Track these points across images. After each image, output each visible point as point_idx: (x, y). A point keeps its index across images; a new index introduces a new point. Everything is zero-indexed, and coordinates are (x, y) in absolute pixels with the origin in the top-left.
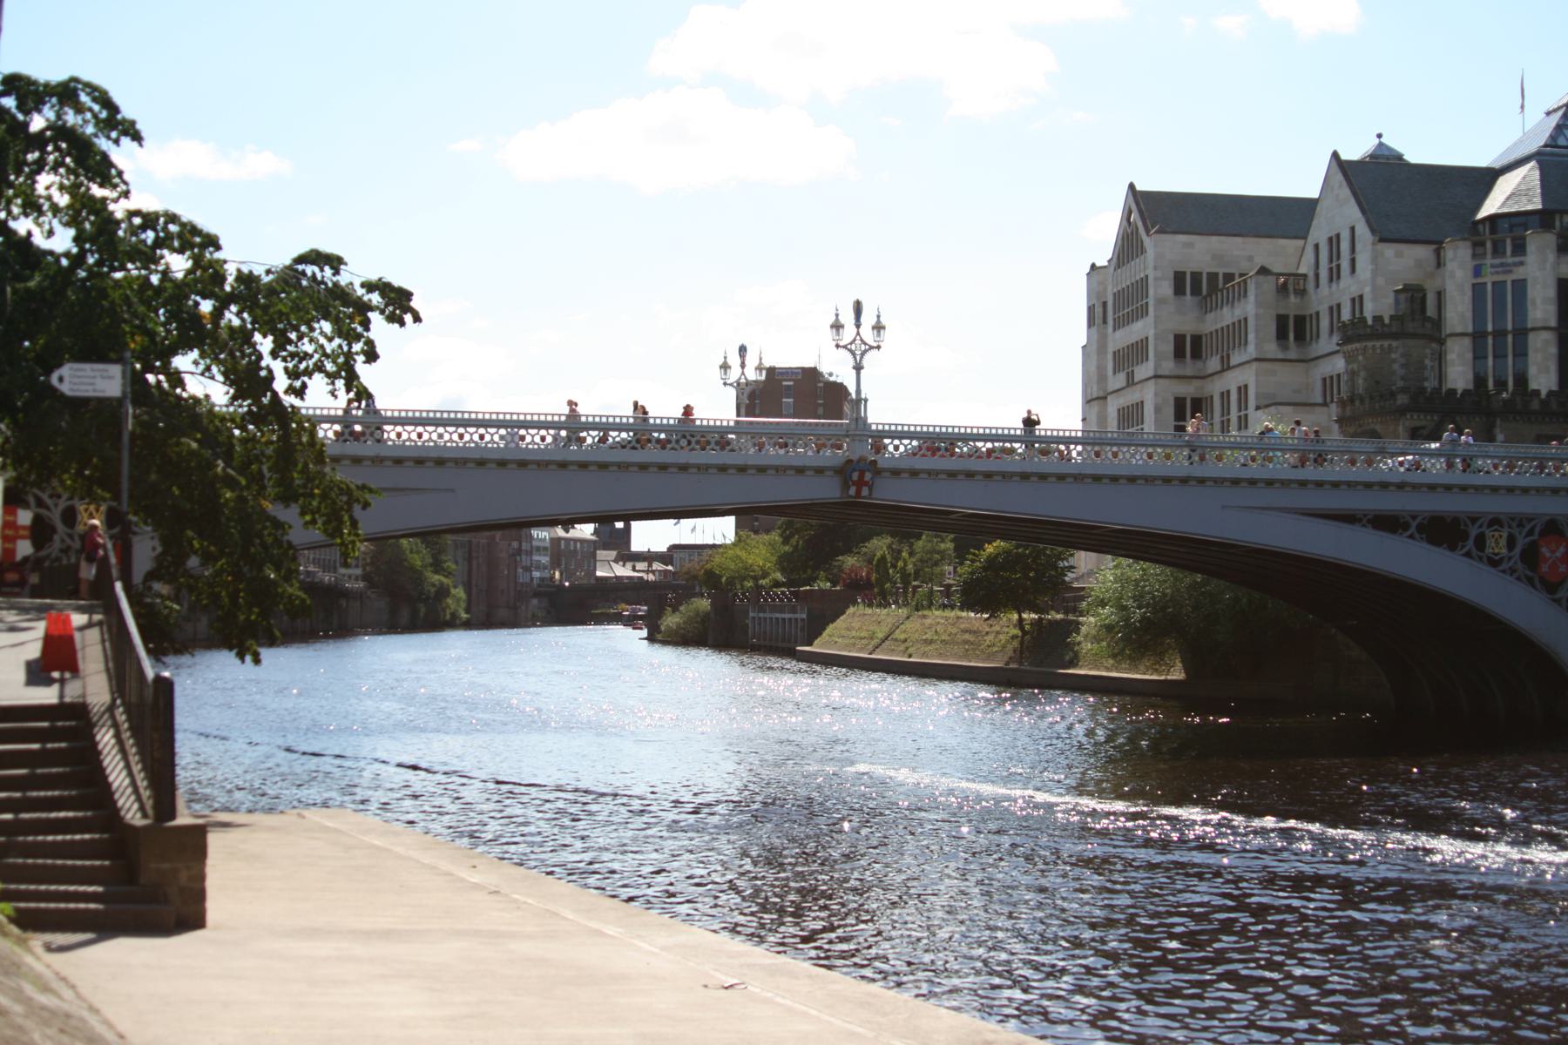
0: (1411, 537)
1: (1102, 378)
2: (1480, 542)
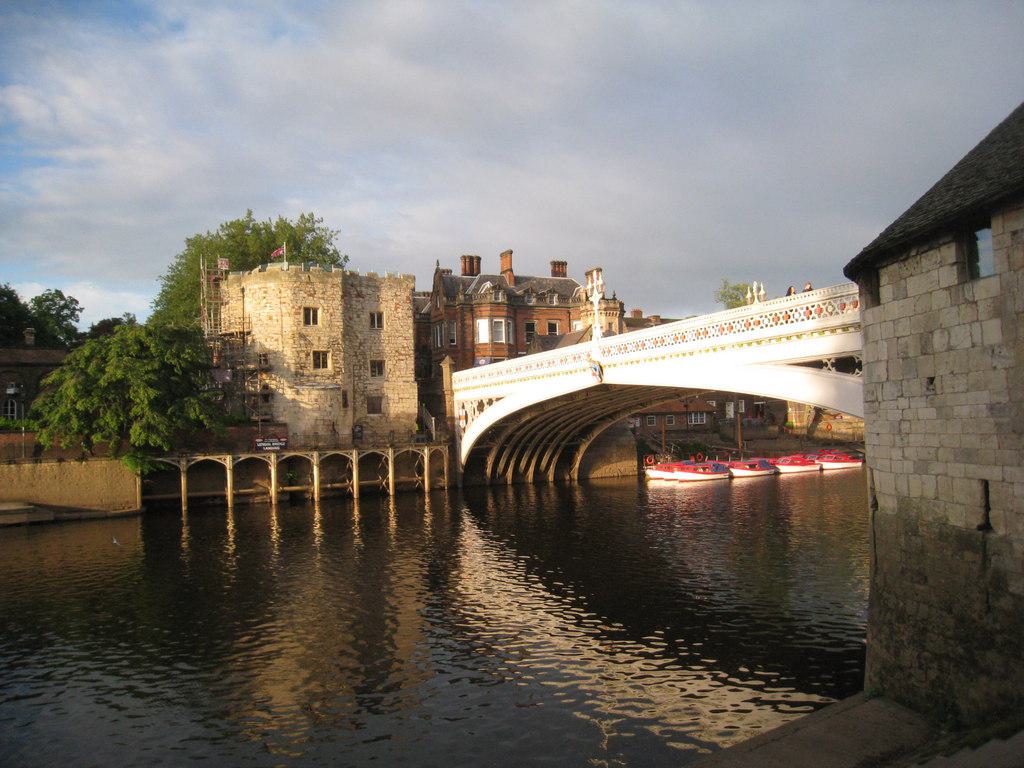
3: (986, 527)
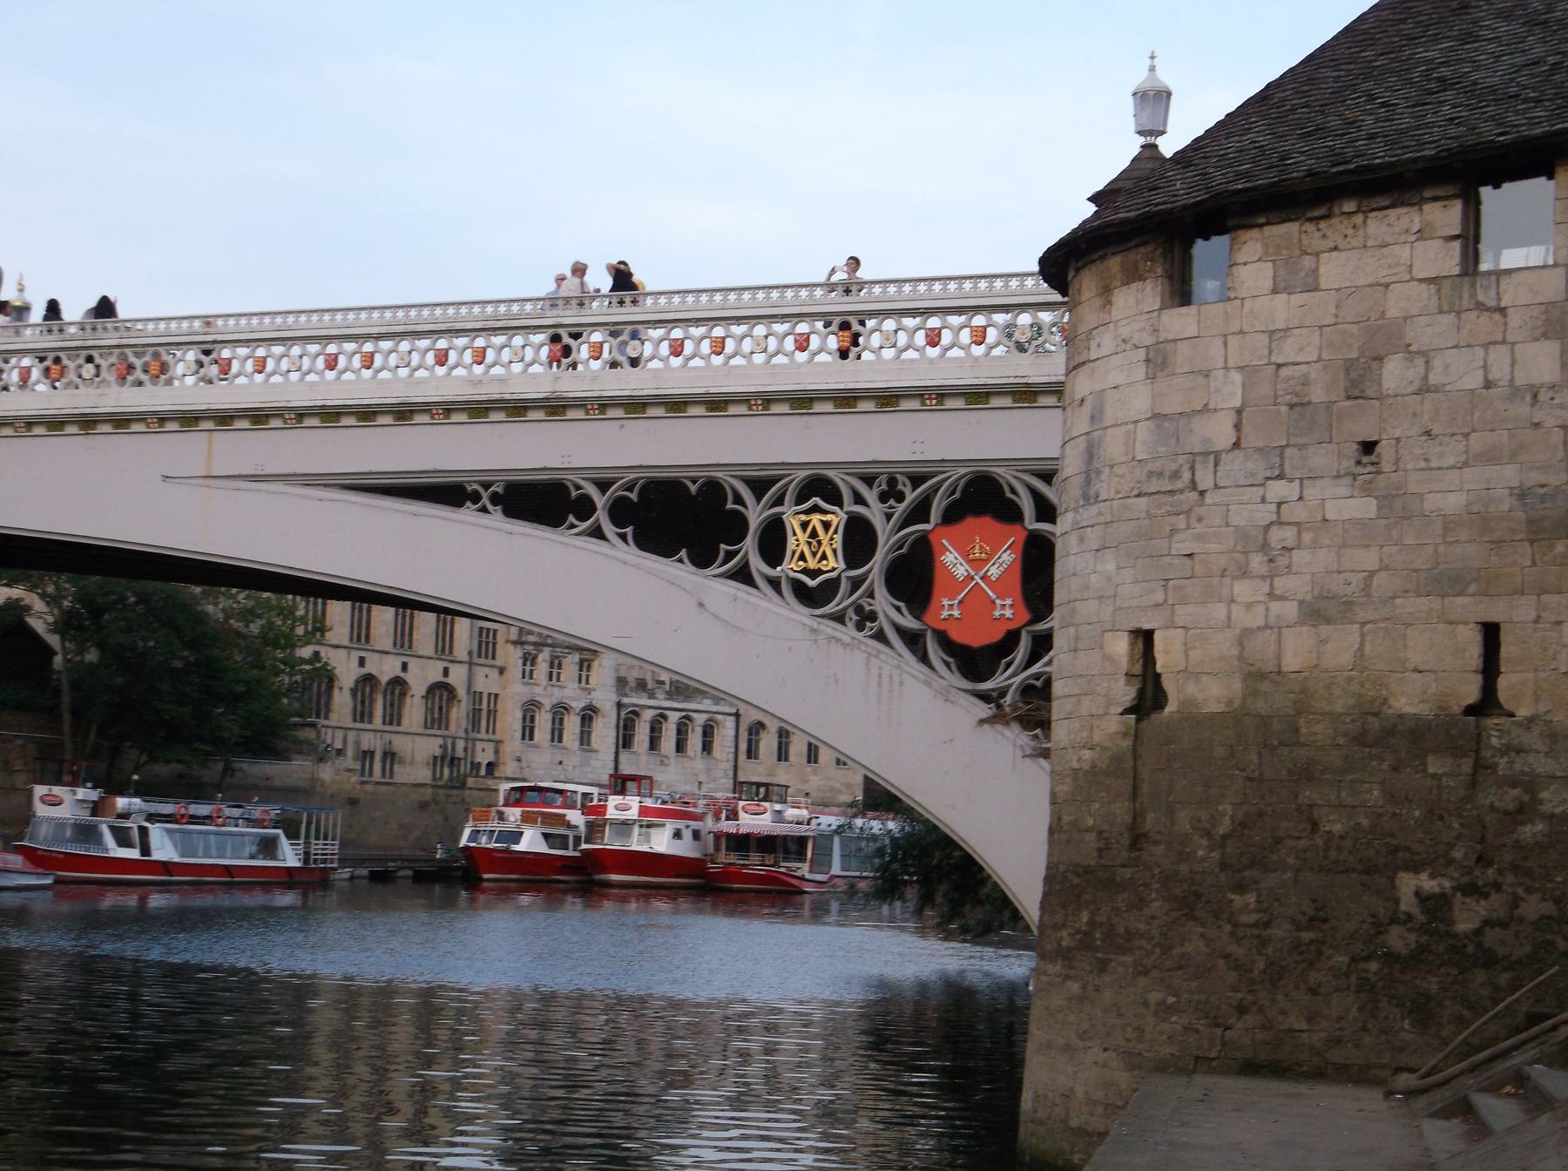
0: (597, 533)
2: (773, 543)
3: (1487, 703)
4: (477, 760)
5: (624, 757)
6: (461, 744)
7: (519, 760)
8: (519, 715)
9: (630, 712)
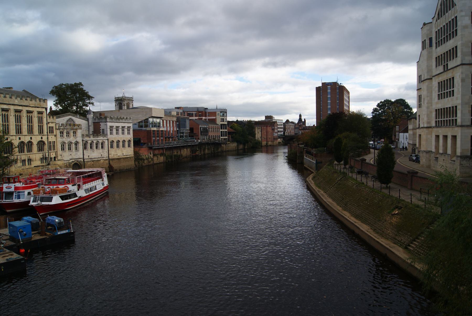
1: (429, 70)
4: (51, 157)
5: (84, 152)
6: (47, 154)
7: (61, 155)
8: (60, 145)
9: (86, 142)
